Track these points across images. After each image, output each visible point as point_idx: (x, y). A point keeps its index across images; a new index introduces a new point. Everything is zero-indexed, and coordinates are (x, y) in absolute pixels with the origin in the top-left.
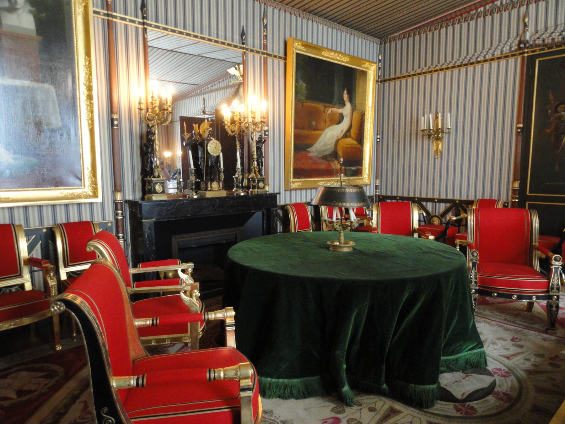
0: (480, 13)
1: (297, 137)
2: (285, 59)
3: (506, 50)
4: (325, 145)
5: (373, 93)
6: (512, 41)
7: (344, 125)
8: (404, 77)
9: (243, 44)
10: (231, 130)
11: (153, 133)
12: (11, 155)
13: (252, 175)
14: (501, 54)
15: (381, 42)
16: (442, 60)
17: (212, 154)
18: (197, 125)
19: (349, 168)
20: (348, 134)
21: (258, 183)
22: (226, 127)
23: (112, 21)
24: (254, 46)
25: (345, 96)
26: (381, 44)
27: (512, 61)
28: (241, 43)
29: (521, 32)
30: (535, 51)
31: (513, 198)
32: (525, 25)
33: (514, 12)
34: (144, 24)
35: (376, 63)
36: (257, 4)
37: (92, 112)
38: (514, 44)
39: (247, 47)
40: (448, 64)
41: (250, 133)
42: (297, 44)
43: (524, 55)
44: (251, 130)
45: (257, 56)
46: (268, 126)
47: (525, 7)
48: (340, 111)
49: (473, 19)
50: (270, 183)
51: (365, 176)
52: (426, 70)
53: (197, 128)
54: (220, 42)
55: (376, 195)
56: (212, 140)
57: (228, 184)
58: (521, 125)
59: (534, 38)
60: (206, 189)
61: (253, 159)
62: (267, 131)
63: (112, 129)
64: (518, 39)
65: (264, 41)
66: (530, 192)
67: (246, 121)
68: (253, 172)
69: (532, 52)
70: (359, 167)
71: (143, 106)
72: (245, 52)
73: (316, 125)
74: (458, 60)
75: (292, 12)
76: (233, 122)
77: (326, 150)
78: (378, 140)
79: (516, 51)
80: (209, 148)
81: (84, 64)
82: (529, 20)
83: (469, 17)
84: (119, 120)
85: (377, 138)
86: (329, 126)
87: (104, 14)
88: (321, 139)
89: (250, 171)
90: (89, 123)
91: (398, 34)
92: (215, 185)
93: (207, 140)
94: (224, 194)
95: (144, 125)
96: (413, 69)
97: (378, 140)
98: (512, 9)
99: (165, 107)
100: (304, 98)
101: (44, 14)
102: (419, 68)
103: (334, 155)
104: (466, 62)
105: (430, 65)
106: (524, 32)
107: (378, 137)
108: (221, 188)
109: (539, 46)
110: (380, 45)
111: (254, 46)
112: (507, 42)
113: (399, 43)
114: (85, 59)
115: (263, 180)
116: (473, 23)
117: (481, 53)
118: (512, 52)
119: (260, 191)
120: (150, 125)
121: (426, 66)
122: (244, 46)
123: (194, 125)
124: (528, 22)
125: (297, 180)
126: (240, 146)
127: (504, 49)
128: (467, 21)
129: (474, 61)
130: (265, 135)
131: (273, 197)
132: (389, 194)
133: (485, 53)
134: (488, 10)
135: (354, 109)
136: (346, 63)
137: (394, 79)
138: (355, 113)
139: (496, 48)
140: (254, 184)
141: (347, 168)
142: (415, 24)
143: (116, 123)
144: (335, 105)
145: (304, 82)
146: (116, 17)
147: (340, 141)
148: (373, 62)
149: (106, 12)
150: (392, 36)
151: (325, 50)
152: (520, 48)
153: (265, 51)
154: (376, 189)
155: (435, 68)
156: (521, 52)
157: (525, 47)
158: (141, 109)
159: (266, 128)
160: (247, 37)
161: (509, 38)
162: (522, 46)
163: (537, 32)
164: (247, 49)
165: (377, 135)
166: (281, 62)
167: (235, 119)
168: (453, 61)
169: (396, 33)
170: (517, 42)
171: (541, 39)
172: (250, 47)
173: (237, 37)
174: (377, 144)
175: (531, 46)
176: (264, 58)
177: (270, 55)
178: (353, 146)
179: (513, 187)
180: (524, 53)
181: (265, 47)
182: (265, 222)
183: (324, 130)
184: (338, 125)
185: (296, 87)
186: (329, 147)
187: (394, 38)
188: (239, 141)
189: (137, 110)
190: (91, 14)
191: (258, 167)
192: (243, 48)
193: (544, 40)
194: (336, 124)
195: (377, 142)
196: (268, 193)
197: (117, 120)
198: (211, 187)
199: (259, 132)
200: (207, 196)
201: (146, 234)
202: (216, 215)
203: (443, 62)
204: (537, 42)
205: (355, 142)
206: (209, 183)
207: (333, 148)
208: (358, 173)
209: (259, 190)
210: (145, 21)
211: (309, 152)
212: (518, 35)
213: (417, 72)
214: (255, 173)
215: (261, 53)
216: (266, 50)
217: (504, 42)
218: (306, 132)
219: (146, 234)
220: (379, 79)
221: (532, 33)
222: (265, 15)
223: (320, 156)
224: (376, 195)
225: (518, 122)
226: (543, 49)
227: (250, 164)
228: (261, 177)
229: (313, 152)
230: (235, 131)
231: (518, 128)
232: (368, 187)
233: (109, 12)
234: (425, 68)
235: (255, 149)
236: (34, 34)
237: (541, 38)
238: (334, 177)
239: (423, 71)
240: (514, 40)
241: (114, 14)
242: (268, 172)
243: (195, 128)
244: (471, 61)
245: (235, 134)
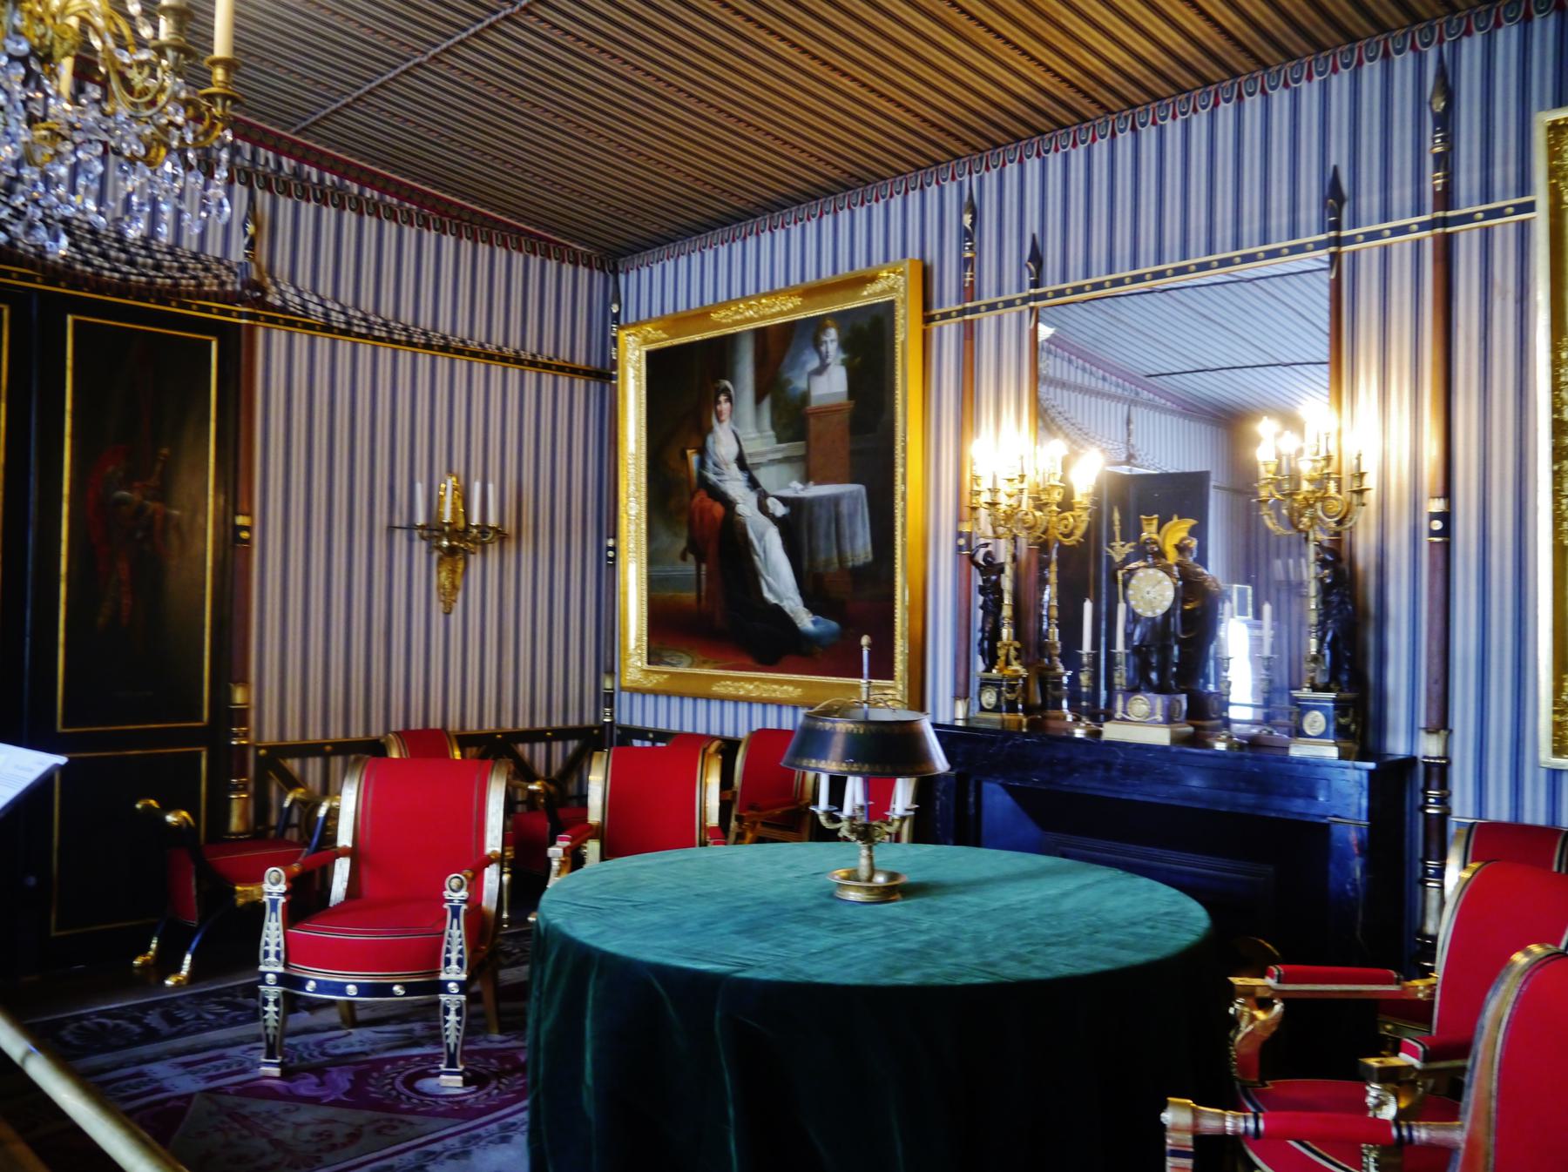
108: (1159, 718)
173: (1310, 211)
177: (1469, 218)
198: (1125, 712)
219: (938, 803)
236: (843, 399)
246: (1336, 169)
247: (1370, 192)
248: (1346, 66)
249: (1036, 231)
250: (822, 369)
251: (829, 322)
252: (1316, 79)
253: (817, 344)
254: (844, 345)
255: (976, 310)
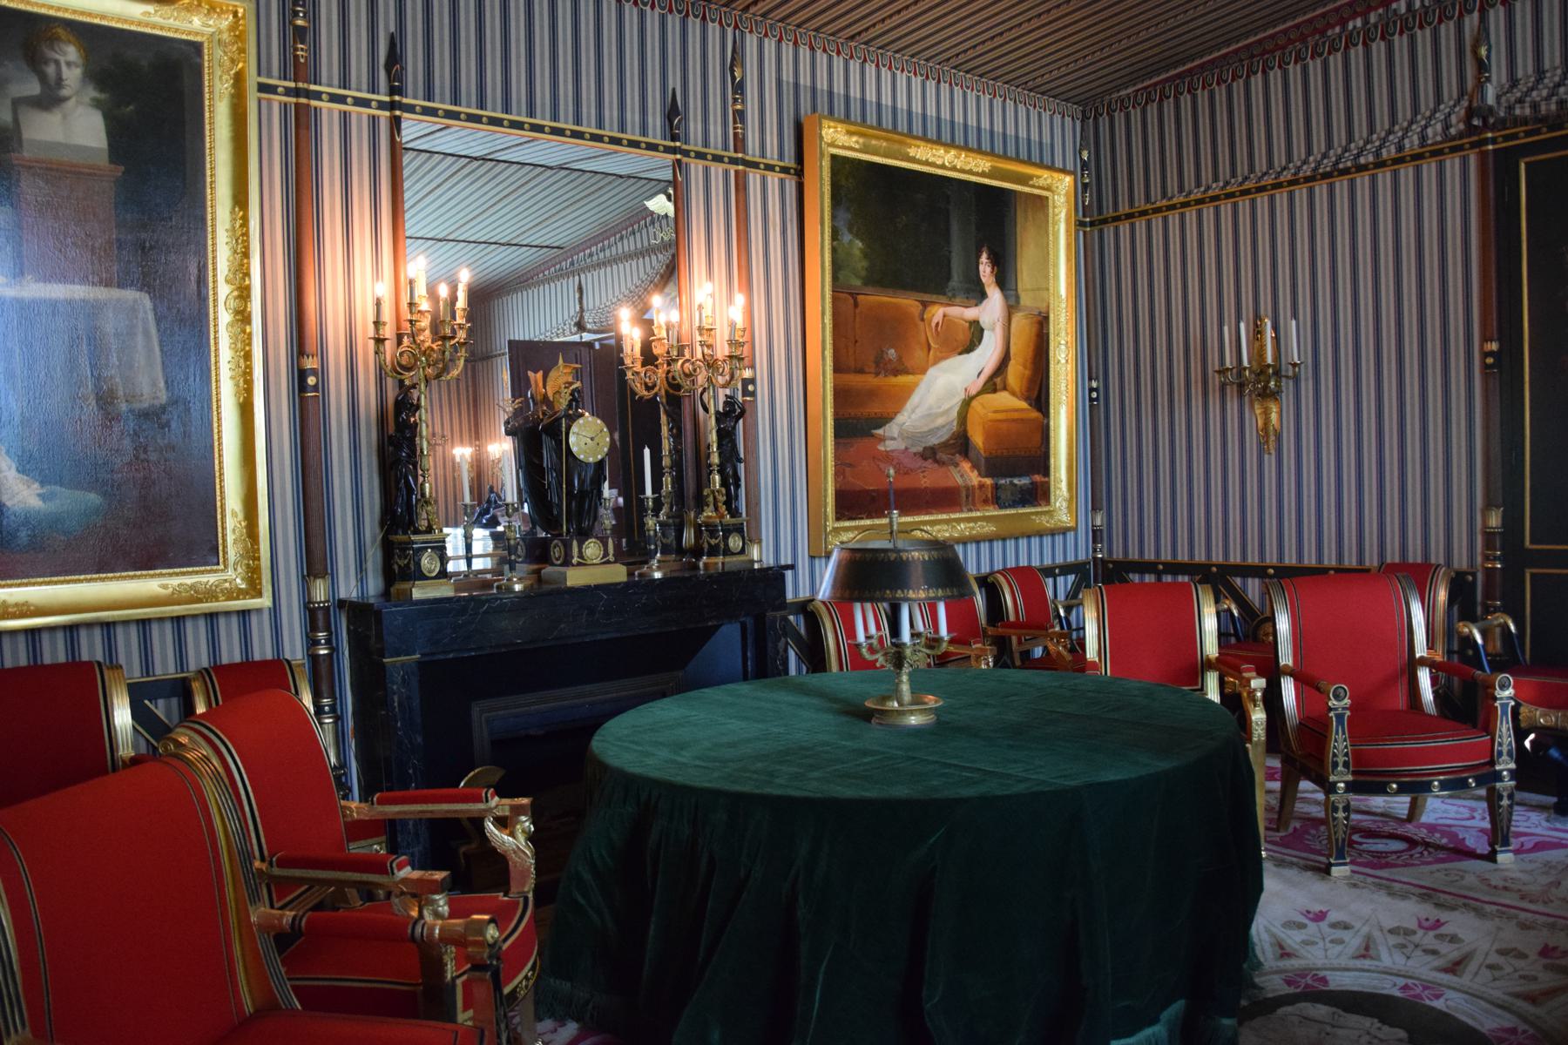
0: (1355, 33)
1: (841, 395)
2: (800, 173)
3: (1435, 134)
4: (930, 416)
5: (1068, 260)
6: (1447, 110)
7: (987, 355)
8: (1157, 210)
9: (674, 138)
10: (646, 384)
11: (412, 404)
12: (36, 485)
13: (709, 512)
14: (1422, 146)
15: (1083, 112)
16: (1261, 164)
17: (582, 457)
18: (540, 375)
19: (1008, 480)
20: (998, 380)
21: (726, 538)
22: (629, 375)
23: (308, 106)
24: (706, 144)
25: (985, 270)
26: (1084, 119)
27: (1453, 164)
28: (668, 135)
29: (1470, 84)
30: (1514, 137)
31: (1486, 558)
32: (1482, 67)
33: (1447, 30)
34: (392, 106)
35: (1073, 173)
36: (714, 28)
37: (248, 356)
38: (1454, 119)
39: (684, 147)
40: (1279, 174)
41: (700, 390)
42: (832, 130)
43: (1484, 148)
44: (701, 379)
45: (717, 170)
46: (753, 367)
47: (1476, 14)
48: (971, 313)
49: (1338, 50)
50: (764, 537)
51: (1058, 504)
52: (1217, 192)
53: (541, 384)
54: (606, 139)
55: (1095, 559)
56: (582, 415)
57: (633, 547)
58: (1494, 346)
59: (1508, 101)
60: (567, 562)
61: (710, 465)
62: (752, 381)
63: (302, 399)
64: (1465, 103)
65: (735, 128)
66: (1532, 542)
67: (687, 356)
68: (712, 507)
69: (1507, 138)
70: (1037, 478)
71: (388, 332)
72: (679, 161)
73: (900, 359)
74: (1305, 162)
75: (818, 45)
76: (649, 358)
77: (933, 432)
78: (1094, 395)
79: (1461, 135)
80: (572, 439)
81: (228, 226)
82: (1489, 51)
83: (1324, 43)
84: (322, 373)
85: (1091, 390)
86: (937, 361)
87: (288, 92)
88: (915, 399)
89: (700, 503)
90: (237, 385)
91: (1130, 90)
92: (592, 549)
93: (568, 416)
94: (617, 574)
95: (390, 384)
96: (1181, 189)
97: (1094, 395)
98: (1440, 21)
99: (448, 331)
100: (858, 283)
101: (131, 107)
102: (1198, 185)
103: (960, 444)
104: (1328, 169)
105: (1228, 178)
106: (1480, 85)
107: (1094, 384)
108: (611, 558)
109: (1524, 121)
110: (1082, 121)
111: (706, 144)
112: (1435, 111)
113: (1135, 115)
114: (232, 212)
115: (739, 529)
116: (1336, 61)
117: (1367, 142)
118: (1450, 141)
119: (733, 562)
120: (407, 382)
121: (1216, 179)
122: (678, 144)
123: (530, 374)
124: (1488, 57)
125: (847, 524)
126: (670, 430)
127: (1430, 131)
128: (1321, 55)
129: (1349, 164)
130: (745, 393)
131: (774, 577)
132: (1134, 555)
133: (1377, 144)
134: (1376, 26)
135: (1012, 306)
136: (983, 174)
137: (1129, 216)
138: (1018, 320)
139: (1406, 130)
140: (713, 542)
141: (1003, 482)
142: (1175, 65)
143: (311, 381)
144: (954, 296)
145: (857, 236)
146: (317, 96)
147: (975, 403)
148: (1064, 171)
149: (292, 85)
150: (1115, 96)
151: (918, 143)
152: (1471, 130)
153: (740, 155)
154: (1095, 541)
155: (1241, 184)
156: (1475, 138)
157: (1486, 126)
158: (379, 341)
159: (747, 374)
160: (686, 118)
161: (1439, 99)
162: (1475, 122)
163: (1514, 82)
164: (686, 153)
165: (1090, 379)
166: (787, 182)
167: (656, 351)
168: (1291, 165)
169: (1126, 88)
170: (1461, 111)
171: (1527, 105)
172: (695, 145)
173: (656, 120)
174: (1091, 406)
175: (1502, 124)
176: (737, 172)
177: (755, 165)
178: (1016, 415)
179: (1485, 525)
180: (1486, 141)
181: (740, 143)
182: (749, 654)
183: (924, 371)
184: (965, 356)
185: (834, 250)
186: (940, 421)
187: (1122, 101)
188: (666, 412)
189: (372, 343)
190: (252, 97)
191: (724, 490)
192: (673, 151)
193: (1535, 106)
194: (960, 354)
195: (1091, 400)
196: (756, 566)
197: (314, 372)
198: (581, 556)
199: (724, 386)
200: (569, 584)
201: (396, 698)
202: (599, 637)
203: (1264, 170)
204: (1518, 112)
205: (1024, 405)
206: (575, 543)
207: (955, 423)
208: (1038, 494)
209: (728, 559)
210: (397, 98)
211: (882, 439)
212: (1462, 92)
213: (1192, 197)
214: (716, 509)
215: (726, 160)
216: (744, 152)
217: (1428, 114)
218: (870, 381)
219: (396, 698)
220: (1084, 216)
221: (1502, 87)
222: (737, 57)
223: (914, 450)
224: (1095, 559)
225: (1485, 339)
226: (1537, 132)
227: (702, 481)
228: (734, 521)
229: (893, 439)
230: (654, 385)
231: (1486, 354)
232: (1071, 535)
233: (300, 85)
234: (1214, 185)
235: (713, 437)
236: (103, 160)
237: (1528, 99)
238: (961, 511)
239: (1210, 193)
240: (1455, 106)
241: (313, 87)
242: (758, 504)
243: (533, 382)
244: (1341, 166)
245: (656, 395)
246: (674, 90)
247: (695, 121)
248: (680, 12)
249: (392, 29)
250: (50, 99)
251: (60, 31)
252: (657, 10)
253: (35, 62)
254: (98, 76)
255: (317, 96)
